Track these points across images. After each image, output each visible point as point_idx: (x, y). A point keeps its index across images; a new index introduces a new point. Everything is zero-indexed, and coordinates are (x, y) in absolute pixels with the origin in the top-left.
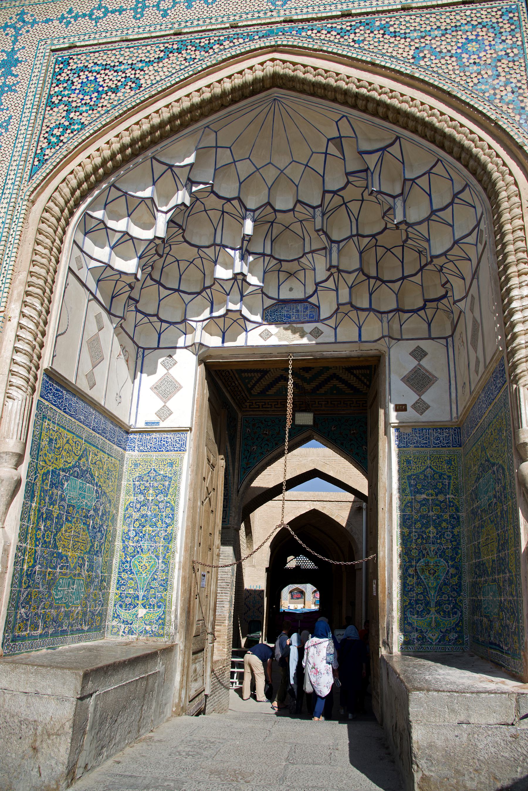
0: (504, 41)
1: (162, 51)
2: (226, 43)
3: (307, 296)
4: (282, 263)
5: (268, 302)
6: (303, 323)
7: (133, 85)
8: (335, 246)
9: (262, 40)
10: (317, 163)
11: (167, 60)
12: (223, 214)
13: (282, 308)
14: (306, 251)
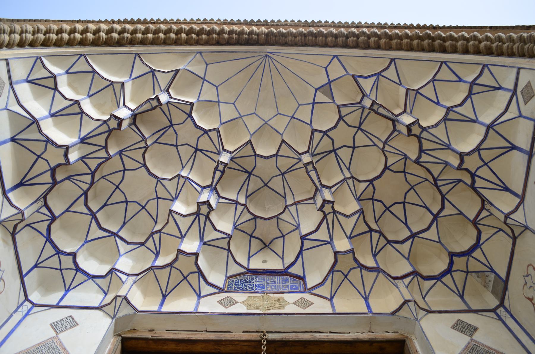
3: (286, 266)
4: (258, 220)
5: (235, 269)
6: (283, 293)
10: (304, 114)
12: (195, 152)
13: (253, 279)
14: (288, 203)
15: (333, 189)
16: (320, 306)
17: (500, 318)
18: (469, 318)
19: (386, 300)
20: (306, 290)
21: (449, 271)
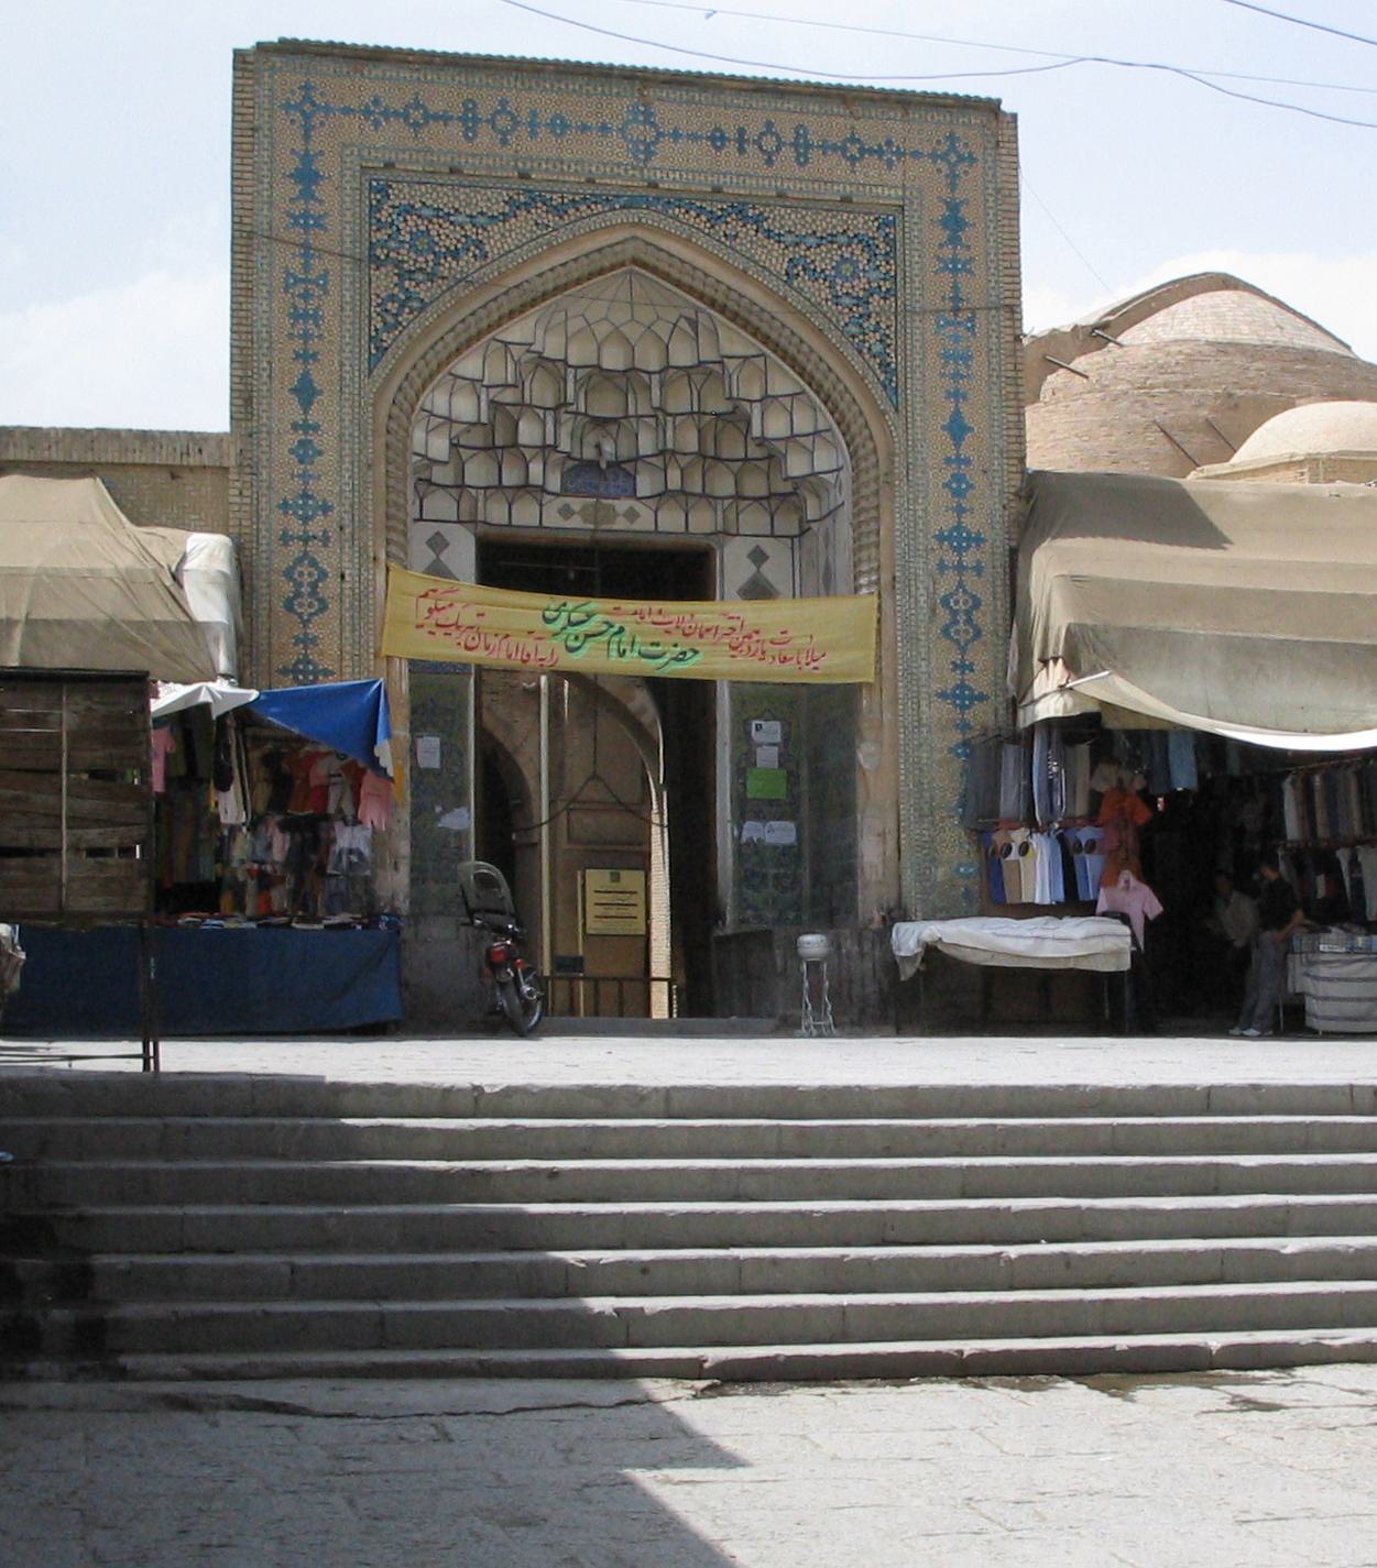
0: (878, 267)
1: (506, 203)
2: (583, 208)
7: (477, 252)
8: (669, 419)
9: (625, 211)
10: (663, 330)
11: (513, 220)
15: (679, 419)
16: (645, 522)
17: (792, 549)
18: (767, 545)
19: (703, 522)
20: (633, 495)
21: (767, 498)
